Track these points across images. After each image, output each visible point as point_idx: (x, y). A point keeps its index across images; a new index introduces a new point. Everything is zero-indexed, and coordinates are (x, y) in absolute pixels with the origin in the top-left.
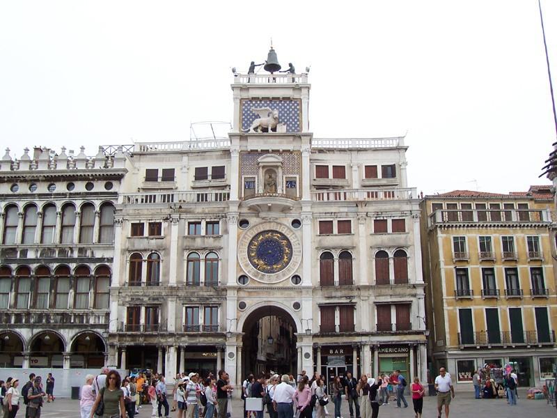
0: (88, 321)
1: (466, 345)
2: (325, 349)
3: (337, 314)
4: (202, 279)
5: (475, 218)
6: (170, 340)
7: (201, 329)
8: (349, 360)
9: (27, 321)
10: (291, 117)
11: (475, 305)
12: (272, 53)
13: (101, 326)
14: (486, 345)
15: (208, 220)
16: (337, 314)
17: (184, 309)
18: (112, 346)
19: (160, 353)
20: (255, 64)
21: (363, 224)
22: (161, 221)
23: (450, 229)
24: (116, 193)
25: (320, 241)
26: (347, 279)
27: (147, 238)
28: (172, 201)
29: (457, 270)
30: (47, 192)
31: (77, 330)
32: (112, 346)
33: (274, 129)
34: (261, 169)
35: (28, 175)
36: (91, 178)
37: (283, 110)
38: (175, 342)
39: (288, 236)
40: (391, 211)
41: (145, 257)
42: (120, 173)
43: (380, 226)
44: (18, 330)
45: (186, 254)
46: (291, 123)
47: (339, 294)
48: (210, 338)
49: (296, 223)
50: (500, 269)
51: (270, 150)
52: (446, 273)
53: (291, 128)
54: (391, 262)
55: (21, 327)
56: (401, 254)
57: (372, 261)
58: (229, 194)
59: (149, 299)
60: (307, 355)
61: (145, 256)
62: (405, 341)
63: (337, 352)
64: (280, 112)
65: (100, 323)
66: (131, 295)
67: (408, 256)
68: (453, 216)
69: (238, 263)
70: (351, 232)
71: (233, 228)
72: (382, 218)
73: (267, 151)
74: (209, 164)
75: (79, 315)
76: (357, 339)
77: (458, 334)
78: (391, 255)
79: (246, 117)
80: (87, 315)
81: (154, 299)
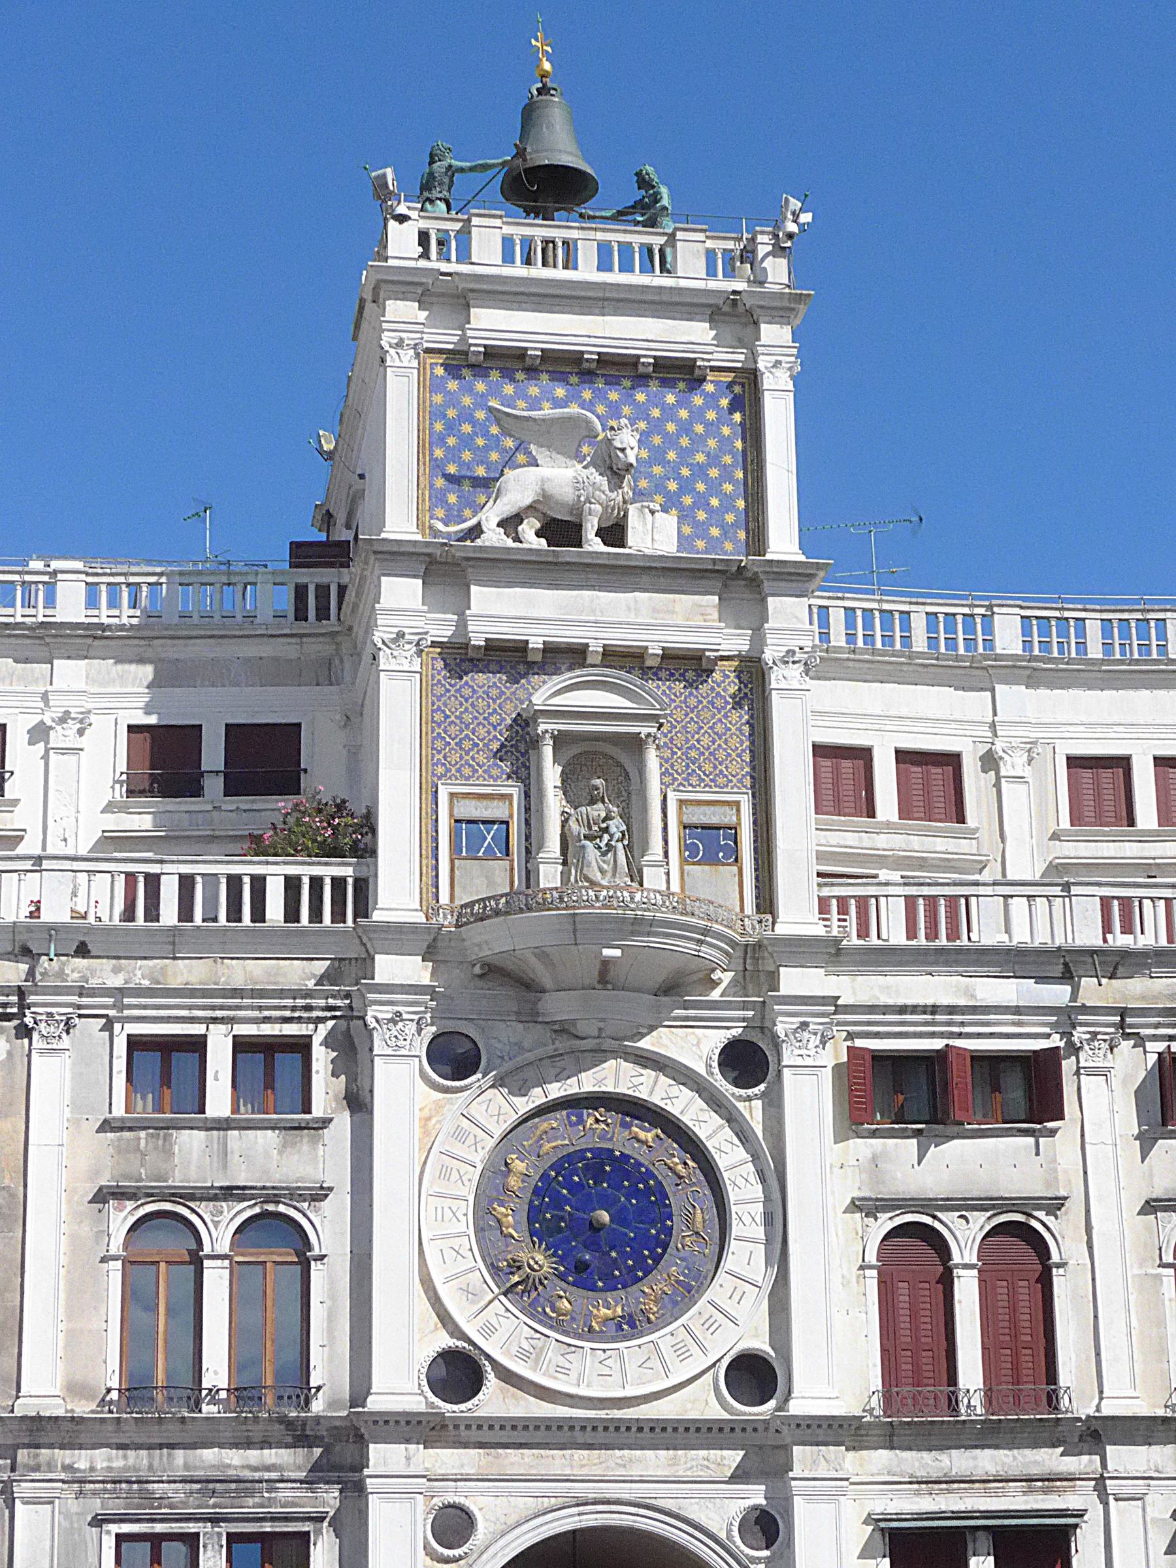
4: (216, 1371)
10: (700, 471)
17: (109, 1543)
21: (1103, 1073)
25: (875, 1160)
33: (614, 533)
34: (548, 751)
37: (656, 426)
39: (702, 1132)
46: (701, 502)
47: (987, 1461)
51: (596, 647)
53: (701, 530)
57: (1159, 1277)
58: (364, 888)
69: (427, 1283)
73: (575, 655)
79: (453, 454)
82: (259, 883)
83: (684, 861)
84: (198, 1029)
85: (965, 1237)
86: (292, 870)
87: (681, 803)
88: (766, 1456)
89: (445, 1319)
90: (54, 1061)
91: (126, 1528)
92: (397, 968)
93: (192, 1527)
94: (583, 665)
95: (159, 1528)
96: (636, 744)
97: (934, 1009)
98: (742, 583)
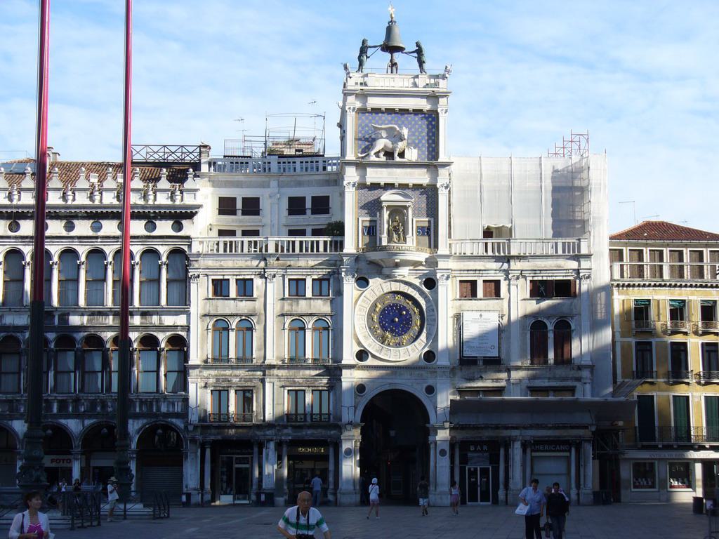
0: (159, 409)
1: (645, 443)
6: (268, 433)
7: (308, 419)
8: (494, 460)
9: (76, 409)
11: (659, 391)
13: (177, 415)
14: (671, 443)
15: (316, 277)
18: (193, 441)
19: (256, 450)
20: (369, 44)
22: (253, 277)
23: (631, 288)
24: (188, 238)
27: (234, 299)
28: (266, 250)
29: (637, 344)
30: (91, 233)
31: (145, 421)
32: (193, 441)
33: (402, 155)
35: (63, 211)
36: (152, 215)
38: (276, 435)
41: (234, 323)
42: (194, 211)
44: (63, 421)
45: (288, 320)
48: (319, 430)
52: (622, 348)
54: (551, 335)
55: (68, 417)
57: (526, 334)
59: (240, 381)
60: (443, 453)
61: (234, 323)
62: (565, 436)
63: (479, 448)
64: (410, 130)
65: (176, 411)
66: (216, 375)
67: (573, 327)
70: (500, 296)
72: (540, 278)
74: (308, 193)
75: (146, 400)
77: (635, 427)
78: (550, 327)
80: (158, 401)
81: (246, 380)
82: (318, 242)
83: (417, 235)
84: (304, 277)
86: (326, 239)
87: (417, 221)
89: (359, 343)
90: (272, 284)
91: (290, 388)
93: (304, 388)
94: (395, 188)
95: (297, 388)
96: (406, 208)
97: (475, 270)
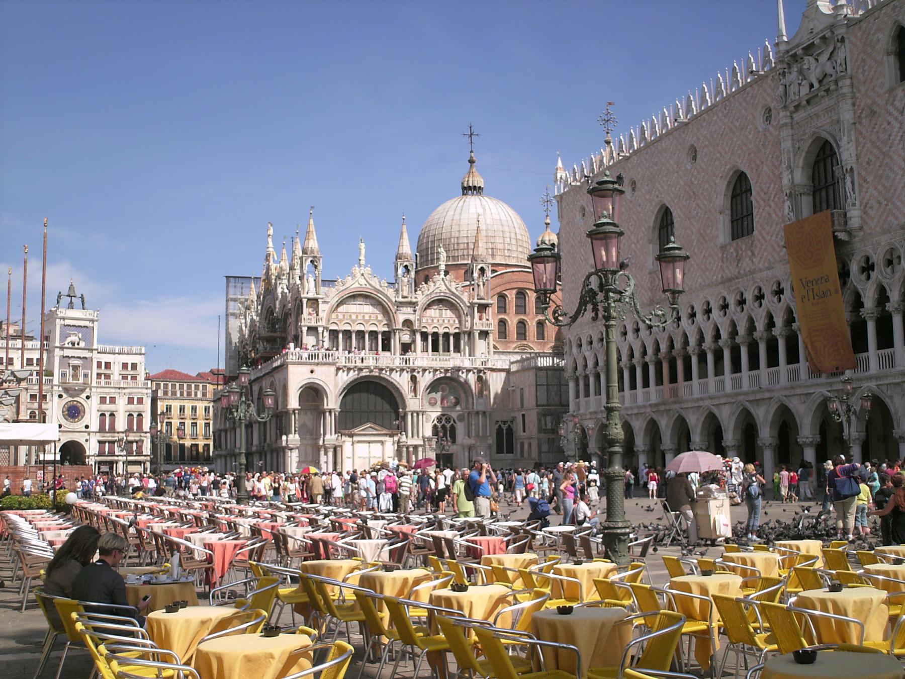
2: (100, 463)
3: (107, 444)
5: (178, 395)
8: (111, 468)
12: (71, 287)
16: (107, 444)
26: (112, 429)
40: (136, 393)
43: (130, 401)
45: (29, 412)
49: (88, 397)
50: (188, 423)
56: (140, 415)
68: (165, 393)
71: (56, 398)
76: (116, 458)
85: (107, 414)
88: (89, 434)
92: (55, 388)
98: (91, 350)
